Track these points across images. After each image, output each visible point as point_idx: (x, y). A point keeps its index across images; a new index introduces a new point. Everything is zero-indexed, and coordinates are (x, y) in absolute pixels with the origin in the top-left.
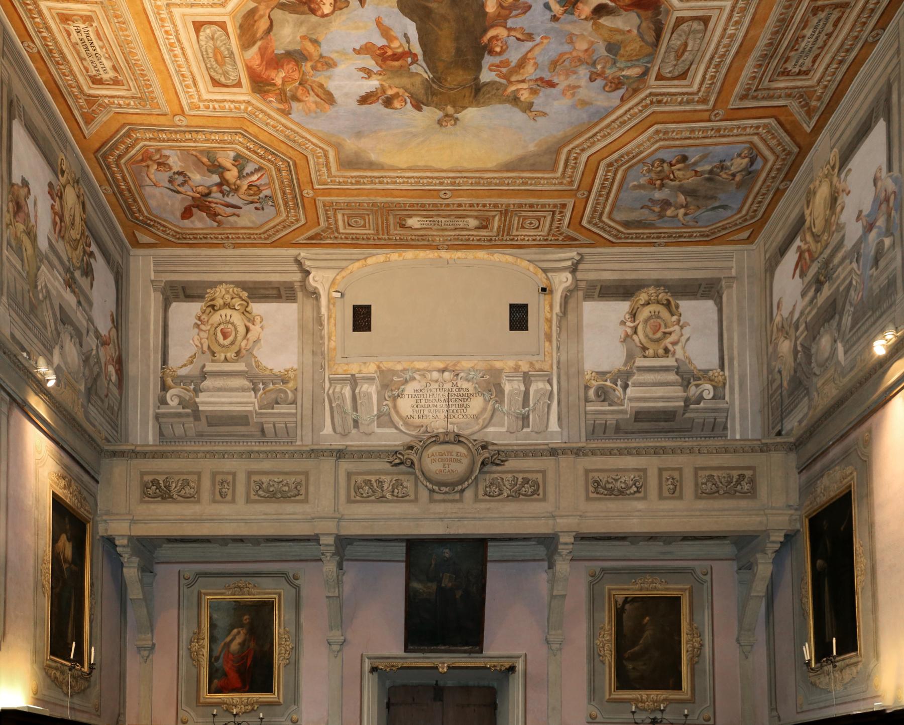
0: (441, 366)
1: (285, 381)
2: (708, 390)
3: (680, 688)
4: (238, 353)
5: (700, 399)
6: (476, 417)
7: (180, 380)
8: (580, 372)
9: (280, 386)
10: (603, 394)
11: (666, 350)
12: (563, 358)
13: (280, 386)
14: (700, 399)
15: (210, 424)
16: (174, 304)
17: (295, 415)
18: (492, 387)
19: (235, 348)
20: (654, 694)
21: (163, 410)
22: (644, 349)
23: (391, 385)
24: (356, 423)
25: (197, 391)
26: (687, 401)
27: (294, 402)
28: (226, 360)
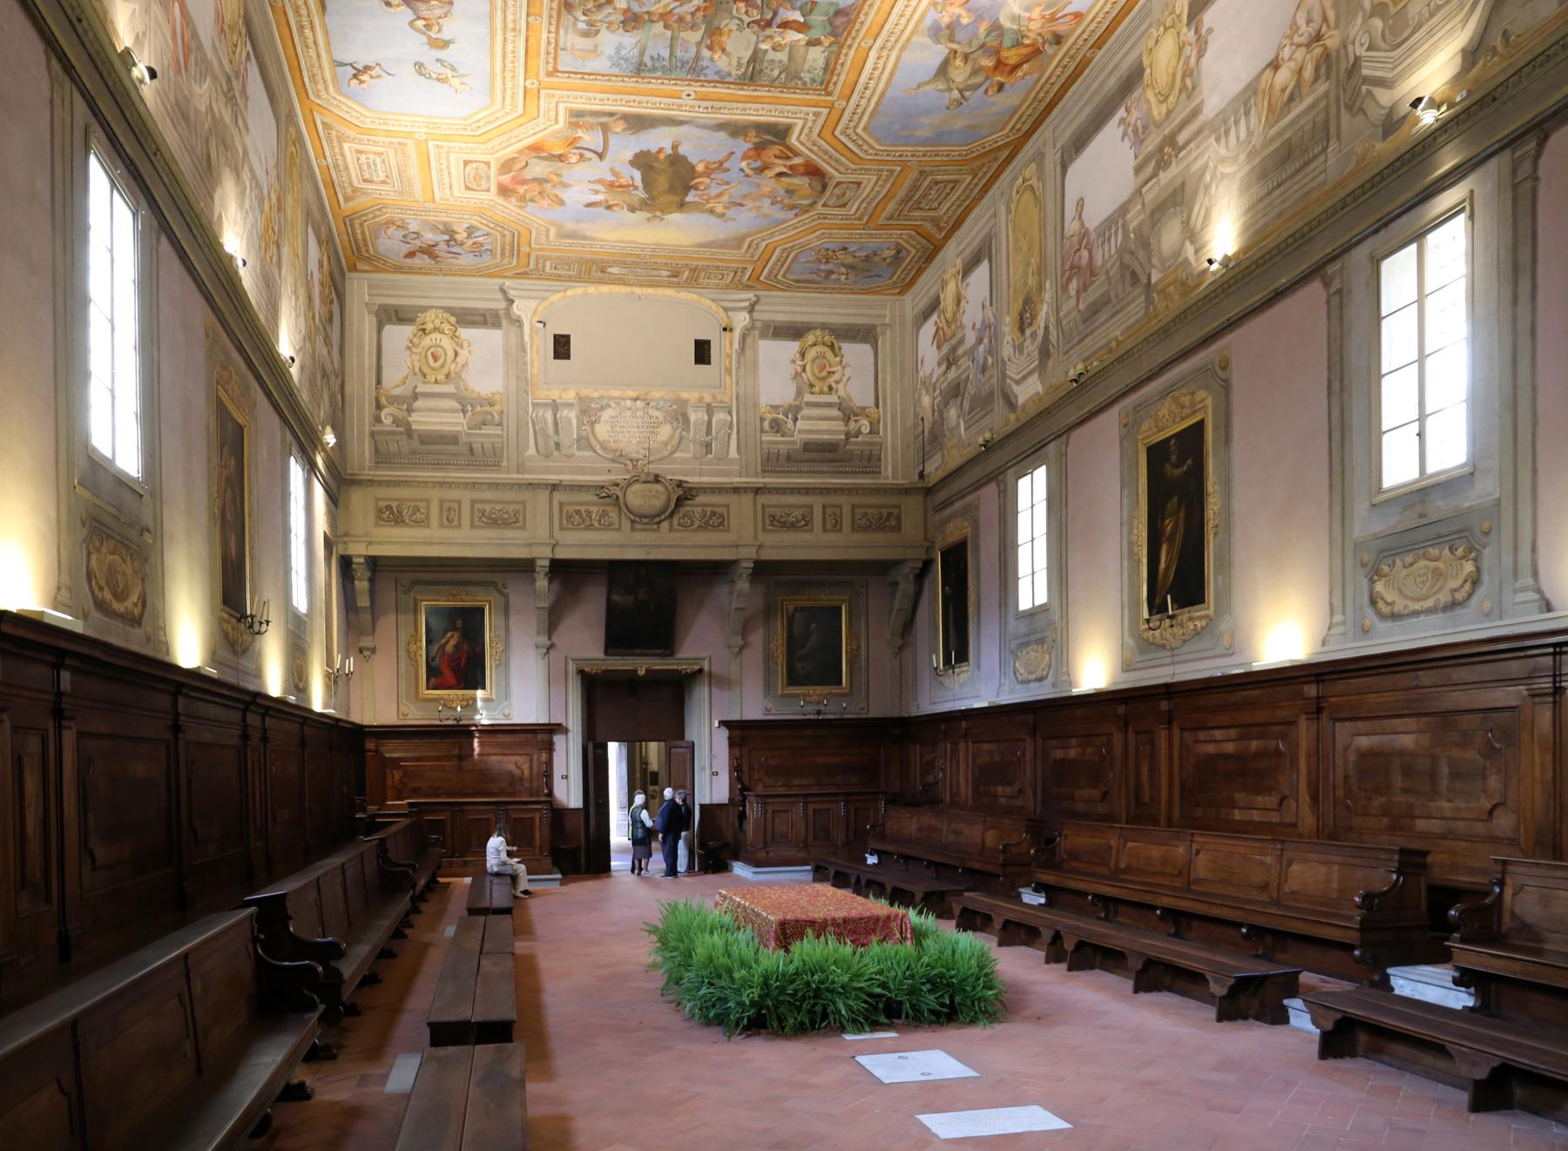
0: (634, 394)
1: (491, 404)
2: (865, 426)
3: (840, 683)
4: (447, 376)
5: (858, 433)
6: (666, 444)
7: (394, 400)
8: (756, 405)
9: (487, 408)
10: (776, 426)
11: (830, 388)
12: (742, 392)
13: (487, 408)
14: (858, 433)
15: (422, 443)
16: (387, 327)
17: (501, 436)
18: (679, 416)
19: (445, 371)
20: (819, 689)
21: (378, 428)
22: (812, 386)
23: (588, 411)
24: (557, 445)
25: (410, 410)
26: (848, 434)
27: (500, 424)
28: (436, 382)
